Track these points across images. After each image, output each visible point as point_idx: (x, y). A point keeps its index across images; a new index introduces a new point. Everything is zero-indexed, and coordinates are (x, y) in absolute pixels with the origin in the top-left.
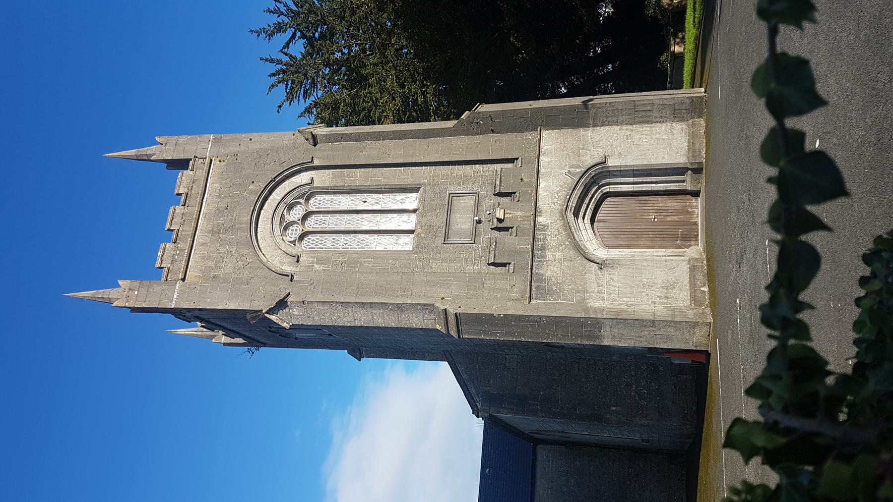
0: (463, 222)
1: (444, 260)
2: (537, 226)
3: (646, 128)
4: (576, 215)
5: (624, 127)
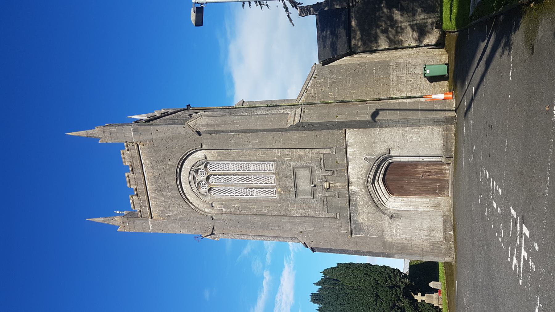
0: (304, 185)
1: (298, 208)
2: (350, 192)
3: (416, 130)
4: (373, 182)
5: (401, 129)
